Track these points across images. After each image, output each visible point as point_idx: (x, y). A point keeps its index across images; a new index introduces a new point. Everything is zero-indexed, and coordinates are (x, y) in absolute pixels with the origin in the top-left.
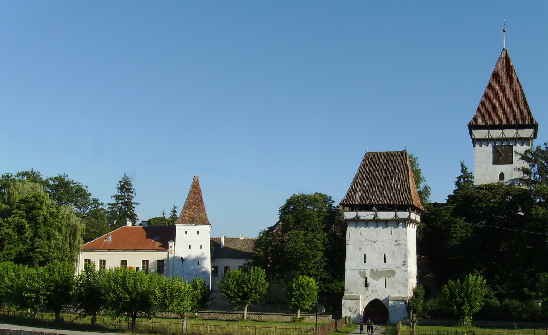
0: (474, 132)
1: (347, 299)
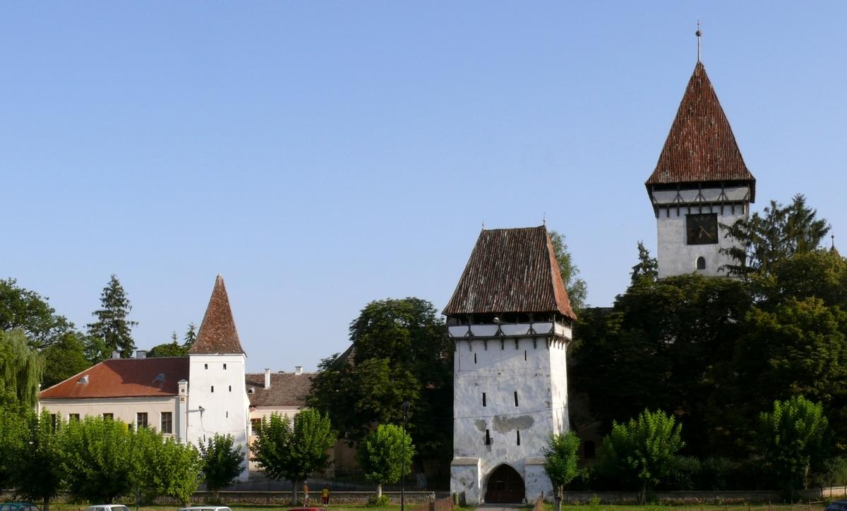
1: (458, 466)
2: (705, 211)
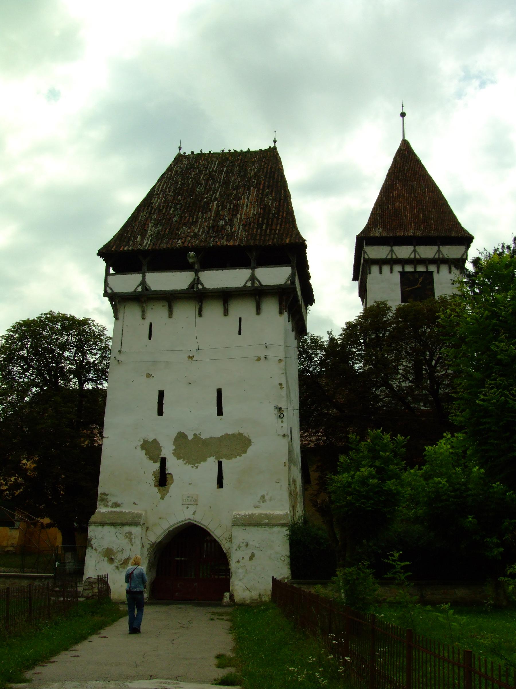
1: (103, 524)
2: (421, 269)
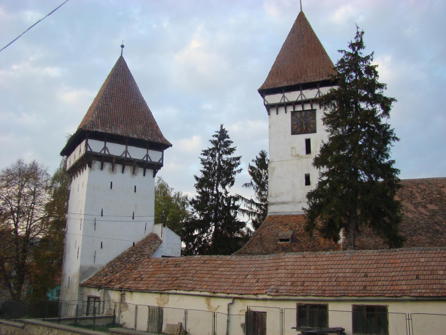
0: (267, 97)
2: (308, 107)
